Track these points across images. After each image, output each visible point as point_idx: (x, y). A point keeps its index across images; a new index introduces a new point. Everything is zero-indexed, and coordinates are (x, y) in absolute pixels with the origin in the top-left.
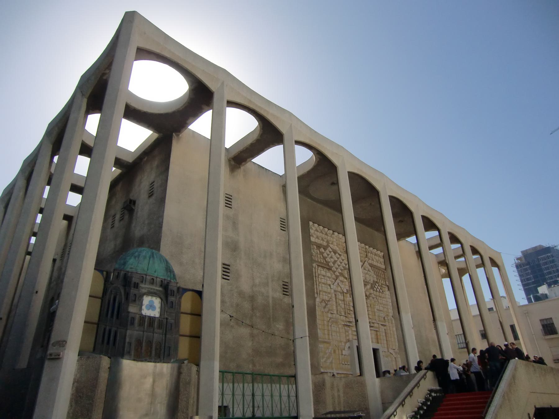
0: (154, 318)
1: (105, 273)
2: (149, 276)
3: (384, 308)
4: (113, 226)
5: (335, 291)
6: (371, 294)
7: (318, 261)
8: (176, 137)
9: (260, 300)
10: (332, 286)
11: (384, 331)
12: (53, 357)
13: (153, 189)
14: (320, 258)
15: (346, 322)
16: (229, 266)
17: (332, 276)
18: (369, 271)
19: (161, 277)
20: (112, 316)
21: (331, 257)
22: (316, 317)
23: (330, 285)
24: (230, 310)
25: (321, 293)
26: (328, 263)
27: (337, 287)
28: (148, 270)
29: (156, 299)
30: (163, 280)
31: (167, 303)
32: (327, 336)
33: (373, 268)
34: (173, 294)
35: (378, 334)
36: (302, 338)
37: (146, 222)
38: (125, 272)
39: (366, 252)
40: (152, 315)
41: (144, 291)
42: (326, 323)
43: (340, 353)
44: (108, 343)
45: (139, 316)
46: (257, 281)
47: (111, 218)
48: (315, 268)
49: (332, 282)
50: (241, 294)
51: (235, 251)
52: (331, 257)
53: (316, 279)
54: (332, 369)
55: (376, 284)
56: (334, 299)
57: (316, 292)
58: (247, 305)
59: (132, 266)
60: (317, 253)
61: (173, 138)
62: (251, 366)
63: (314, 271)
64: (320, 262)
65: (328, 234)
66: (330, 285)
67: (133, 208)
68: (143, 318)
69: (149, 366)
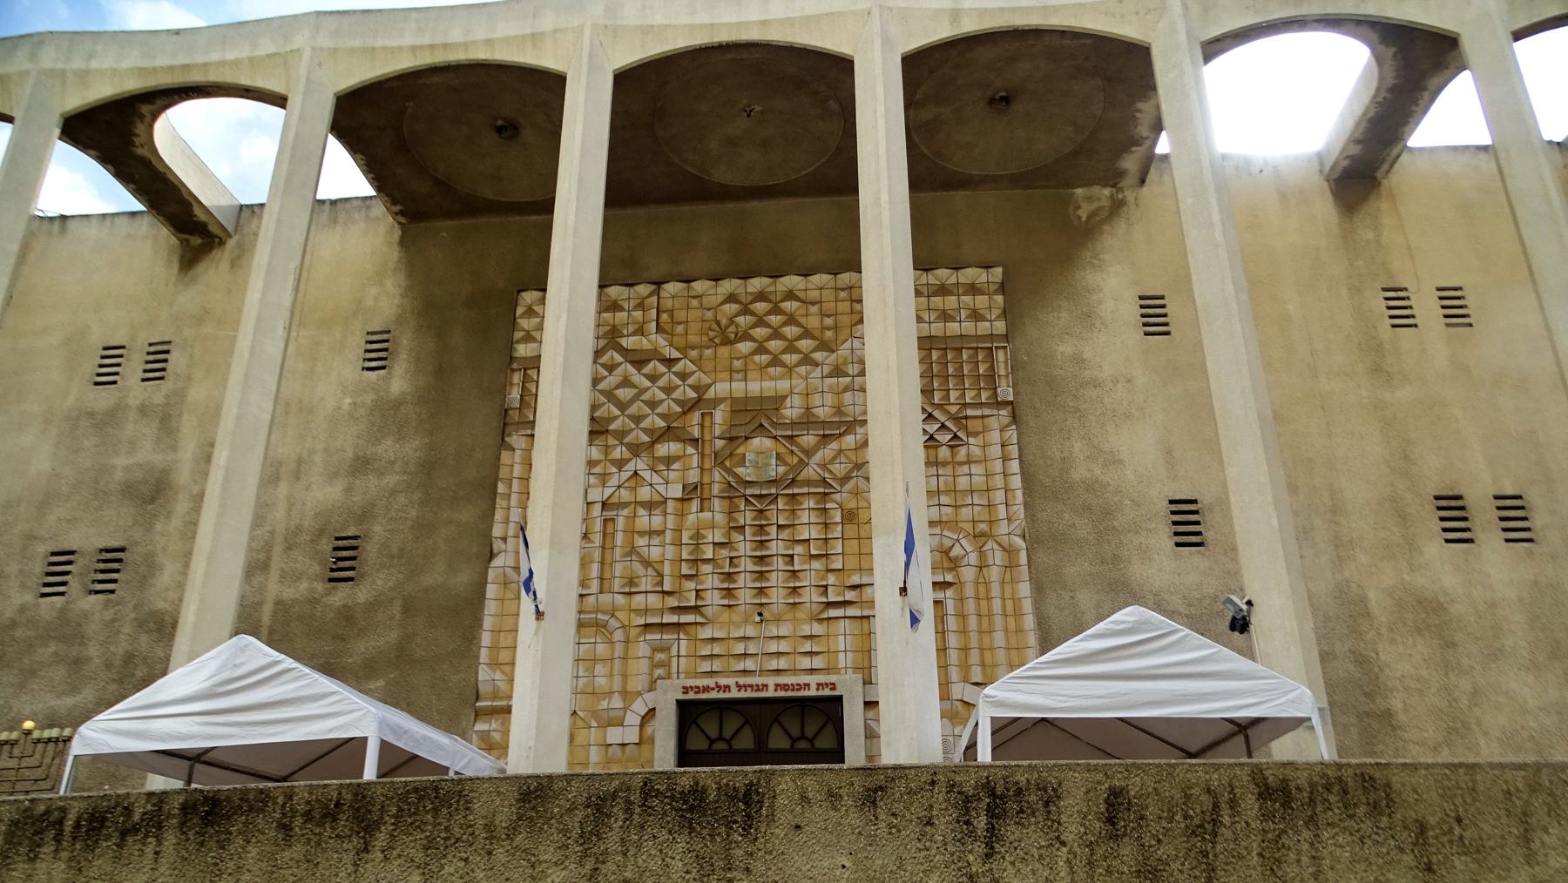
3: (956, 507)
15: (662, 612)
27: (634, 489)
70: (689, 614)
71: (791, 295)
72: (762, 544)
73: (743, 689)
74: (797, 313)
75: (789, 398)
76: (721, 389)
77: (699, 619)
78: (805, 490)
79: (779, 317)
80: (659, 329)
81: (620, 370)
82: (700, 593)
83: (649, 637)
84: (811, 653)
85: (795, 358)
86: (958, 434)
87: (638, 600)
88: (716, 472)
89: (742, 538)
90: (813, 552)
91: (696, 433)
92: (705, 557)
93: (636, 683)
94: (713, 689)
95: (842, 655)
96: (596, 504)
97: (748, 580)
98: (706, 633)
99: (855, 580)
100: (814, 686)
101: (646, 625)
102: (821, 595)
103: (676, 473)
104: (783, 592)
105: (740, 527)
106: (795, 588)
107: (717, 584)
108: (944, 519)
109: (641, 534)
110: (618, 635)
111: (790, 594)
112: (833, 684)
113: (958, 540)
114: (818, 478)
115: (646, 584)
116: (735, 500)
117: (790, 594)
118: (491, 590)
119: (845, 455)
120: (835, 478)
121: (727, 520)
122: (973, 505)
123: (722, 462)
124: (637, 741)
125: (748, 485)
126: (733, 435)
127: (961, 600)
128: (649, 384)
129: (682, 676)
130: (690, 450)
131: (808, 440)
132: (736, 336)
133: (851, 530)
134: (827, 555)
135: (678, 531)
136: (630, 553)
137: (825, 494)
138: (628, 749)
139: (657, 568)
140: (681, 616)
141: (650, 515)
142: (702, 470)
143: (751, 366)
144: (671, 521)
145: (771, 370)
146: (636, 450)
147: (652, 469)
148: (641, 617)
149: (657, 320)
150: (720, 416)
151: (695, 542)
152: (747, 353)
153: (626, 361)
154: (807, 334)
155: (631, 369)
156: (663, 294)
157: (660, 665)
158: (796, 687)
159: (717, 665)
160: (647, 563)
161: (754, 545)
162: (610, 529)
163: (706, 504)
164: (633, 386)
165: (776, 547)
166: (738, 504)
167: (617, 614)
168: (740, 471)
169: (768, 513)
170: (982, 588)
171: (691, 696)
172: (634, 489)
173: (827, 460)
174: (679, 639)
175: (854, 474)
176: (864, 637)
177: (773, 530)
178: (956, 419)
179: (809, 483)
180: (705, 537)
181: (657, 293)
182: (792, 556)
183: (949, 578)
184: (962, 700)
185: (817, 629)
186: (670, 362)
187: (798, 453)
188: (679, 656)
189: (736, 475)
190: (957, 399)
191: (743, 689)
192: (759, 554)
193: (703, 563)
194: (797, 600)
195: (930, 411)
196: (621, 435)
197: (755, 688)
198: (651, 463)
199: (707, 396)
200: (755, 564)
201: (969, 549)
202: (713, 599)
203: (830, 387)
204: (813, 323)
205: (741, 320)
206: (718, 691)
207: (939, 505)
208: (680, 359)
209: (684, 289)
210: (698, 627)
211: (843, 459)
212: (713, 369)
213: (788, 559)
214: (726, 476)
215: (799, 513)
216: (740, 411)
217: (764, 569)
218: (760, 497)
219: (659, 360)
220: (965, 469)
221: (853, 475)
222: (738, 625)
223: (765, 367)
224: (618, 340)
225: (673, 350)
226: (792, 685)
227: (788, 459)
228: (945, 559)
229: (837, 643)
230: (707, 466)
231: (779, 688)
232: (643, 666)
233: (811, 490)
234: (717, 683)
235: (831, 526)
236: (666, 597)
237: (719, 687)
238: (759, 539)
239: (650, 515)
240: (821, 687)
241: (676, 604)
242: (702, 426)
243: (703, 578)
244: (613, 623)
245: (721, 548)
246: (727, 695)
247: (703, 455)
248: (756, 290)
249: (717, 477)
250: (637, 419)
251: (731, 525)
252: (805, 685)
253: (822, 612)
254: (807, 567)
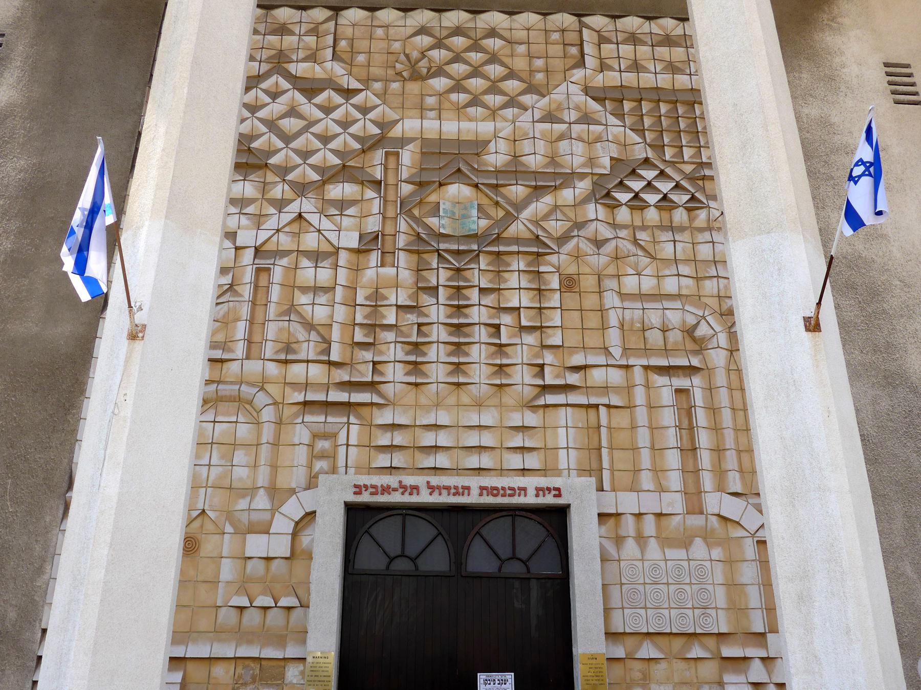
3: (698, 279)
15: (327, 388)
27: (297, 235)
70: (363, 392)
71: (492, 33)
72: (459, 309)
73: (437, 491)
74: (501, 52)
75: (493, 141)
76: (410, 126)
77: (376, 399)
78: (514, 248)
79: (479, 55)
80: (335, 57)
82: (378, 366)
83: (308, 418)
84: (522, 449)
85: (499, 100)
86: (696, 194)
87: (297, 371)
88: (403, 221)
90: (524, 323)
91: (378, 174)
92: (385, 322)
93: (297, 477)
94: (395, 490)
95: (562, 454)
96: (248, 250)
97: (442, 353)
98: (385, 417)
99: (578, 359)
100: (531, 492)
101: (305, 403)
102: (535, 376)
103: (352, 219)
104: (487, 370)
105: (430, 288)
106: (501, 366)
107: (401, 356)
108: (684, 292)
109: (304, 290)
110: (268, 414)
111: (495, 373)
112: (558, 489)
113: (704, 317)
114: (527, 235)
115: (308, 350)
116: (425, 256)
117: (495, 373)
119: (561, 211)
120: (550, 236)
121: (414, 279)
122: (718, 277)
123: (410, 210)
124: (288, 555)
125: (441, 239)
126: (424, 179)
127: (710, 389)
128: (322, 116)
129: (351, 471)
130: (370, 194)
131: (518, 191)
132: (428, 72)
133: (571, 300)
134: (541, 327)
135: (352, 289)
136: (288, 312)
137: (538, 255)
138: (275, 564)
139: (321, 331)
140: (352, 395)
141: (316, 267)
142: (384, 218)
143: (446, 105)
144: (343, 276)
145: (471, 110)
146: (301, 189)
147: (321, 213)
148: (301, 392)
149: (334, 47)
150: (408, 156)
151: (374, 304)
152: (442, 91)
153: (294, 88)
154: (512, 75)
155: (299, 98)
156: (341, 21)
157: (322, 456)
158: (509, 492)
159: (398, 460)
160: (310, 326)
161: (450, 310)
162: (263, 282)
163: (389, 258)
164: (300, 116)
165: (476, 315)
166: (429, 260)
167: (267, 386)
168: (433, 221)
169: (467, 274)
170: (733, 376)
171: (365, 498)
172: (297, 235)
173: (540, 215)
174: (349, 424)
175: (575, 233)
176: (590, 430)
177: (474, 295)
178: (691, 178)
179: (517, 240)
180: (386, 298)
181: (336, 17)
182: (497, 327)
183: (695, 362)
184: (719, 515)
185: (531, 419)
186: (348, 93)
187: (505, 205)
188: (348, 445)
189: (426, 226)
190: (691, 157)
191: (437, 491)
192: (455, 321)
193: (383, 330)
194: (504, 381)
195: (662, 168)
196: (283, 171)
197: (453, 491)
198: (320, 206)
199: (392, 134)
200: (451, 334)
201: (718, 328)
202: (395, 374)
203: (543, 133)
204: (520, 64)
205: (435, 54)
206: (403, 494)
207: (678, 275)
208: (362, 90)
209: (368, 17)
210: (375, 409)
211: (560, 216)
212: (401, 106)
213: (492, 330)
214: (415, 226)
215: (506, 275)
216: (433, 153)
217: (462, 340)
218: (458, 253)
219: (333, 89)
220: (707, 236)
221: (572, 234)
222: (427, 409)
223: (462, 108)
224: (285, 65)
225: (352, 80)
226: (503, 488)
227: (492, 211)
228: (688, 340)
229: (556, 436)
230: (391, 213)
231: (485, 492)
232: (301, 455)
233: (521, 249)
234: (400, 482)
235: (545, 293)
236: (332, 368)
237: (403, 488)
238: (456, 303)
239: (316, 267)
240: (541, 493)
241: (346, 378)
242: (386, 169)
243: (383, 348)
244: (261, 399)
245: (406, 313)
246: (414, 499)
247: (386, 201)
248: (453, 26)
249: (403, 226)
250: (305, 154)
251: (420, 285)
252: (520, 489)
253: (537, 397)
254: (518, 341)
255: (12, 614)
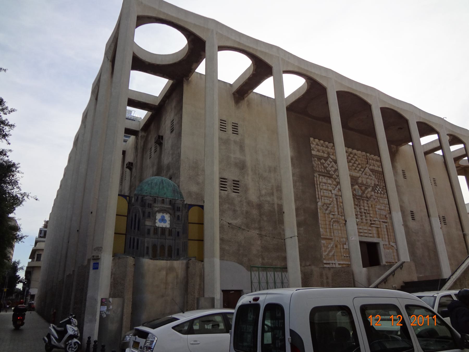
0: (165, 229)
1: (128, 198)
2: (160, 197)
3: (385, 207)
4: (151, 157)
5: (336, 195)
6: (372, 195)
7: (319, 171)
8: (186, 81)
9: (266, 207)
10: (333, 192)
11: (385, 227)
12: (95, 258)
13: (174, 126)
14: (321, 168)
16: (238, 181)
17: (333, 183)
18: (370, 175)
19: (170, 198)
20: (135, 229)
21: (332, 167)
22: (319, 218)
23: (331, 191)
24: (240, 217)
25: (323, 198)
26: (328, 172)
27: (338, 192)
28: (159, 192)
29: (167, 214)
30: (172, 200)
31: (175, 216)
32: (328, 234)
33: (374, 173)
34: (179, 209)
35: (380, 229)
36: (291, 237)
37: (171, 153)
38: (142, 196)
39: (367, 159)
40: (164, 226)
41: (156, 209)
42: (327, 223)
43: (342, 247)
44: (133, 248)
45: (154, 227)
46: (263, 192)
47: (149, 151)
48: (317, 177)
49: (333, 187)
50: (249, 203)
51: (243, 169)
52: (332, 167)
53: (317, 186)
54: (334, 260)
55: (378, 187)
56: (335, 202)
57: (317, 197)
58: (255, 212)
59: (147, 191)
60: (318, 164)
61: (184, 83)
62: (260, 260)
63: (315, 179)
64: (322, 172)
65: (329, 147)
66: (331, 191)
67: (162, 142)
68: (156, 229)
69: (162, 263)
81: (332, 163)
89: (357, 207)
118: (319, 210)
169: (360, 203)
185: (370, 228)
204: (360, 162)
255: (319, 256)
